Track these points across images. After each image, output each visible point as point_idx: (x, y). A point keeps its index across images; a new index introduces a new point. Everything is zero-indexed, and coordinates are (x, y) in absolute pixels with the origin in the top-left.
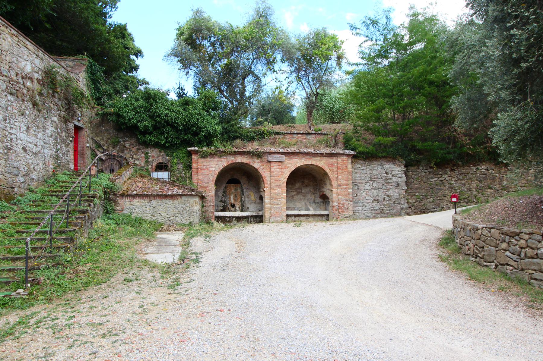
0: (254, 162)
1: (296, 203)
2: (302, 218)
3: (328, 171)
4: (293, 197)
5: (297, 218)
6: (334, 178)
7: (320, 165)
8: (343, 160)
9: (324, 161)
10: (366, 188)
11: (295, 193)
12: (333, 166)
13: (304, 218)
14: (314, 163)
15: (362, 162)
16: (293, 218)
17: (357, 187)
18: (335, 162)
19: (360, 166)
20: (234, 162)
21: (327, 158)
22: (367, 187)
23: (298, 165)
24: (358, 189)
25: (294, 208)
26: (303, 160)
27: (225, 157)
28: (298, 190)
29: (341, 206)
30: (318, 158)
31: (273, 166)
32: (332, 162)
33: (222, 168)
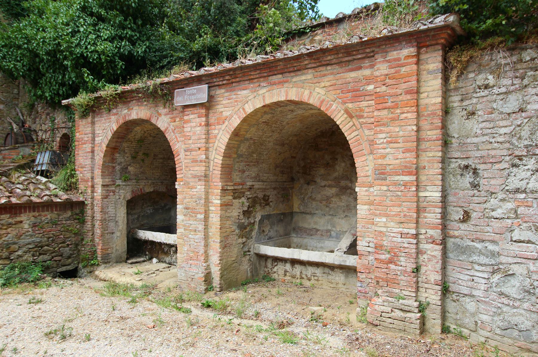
0: (160, 115)
1: (336, 219)
2: (310, 270)
3: (340, 119)
4: (328, 199)
5: (298, 269)
6: (365, 146)
7: (314, 101)
8: (397, 64)
9: (326, 81)
10: (514, 183)
11: (334, 190)
12: (358, 95)
13: (318, 271)
14: (293, 95)
15: (501, 57)
16: (288, 266)
17: (468, 178)
18: (369, 80)
19: (491, 79)
20: (127, 119)
21: (336, 68)
22: (520, 177)
23: (249, 109)
24: (475, 186)
25: (328, 231)
26: (262, 91)
27: (114, 111)
28: (343, 183)
29: (385, 257)
30: (308, 76)
31: (189, 121)
32: (357, 81)
33: (110, 135)
